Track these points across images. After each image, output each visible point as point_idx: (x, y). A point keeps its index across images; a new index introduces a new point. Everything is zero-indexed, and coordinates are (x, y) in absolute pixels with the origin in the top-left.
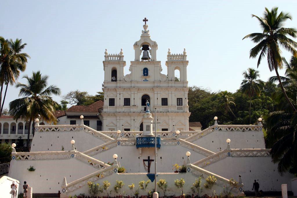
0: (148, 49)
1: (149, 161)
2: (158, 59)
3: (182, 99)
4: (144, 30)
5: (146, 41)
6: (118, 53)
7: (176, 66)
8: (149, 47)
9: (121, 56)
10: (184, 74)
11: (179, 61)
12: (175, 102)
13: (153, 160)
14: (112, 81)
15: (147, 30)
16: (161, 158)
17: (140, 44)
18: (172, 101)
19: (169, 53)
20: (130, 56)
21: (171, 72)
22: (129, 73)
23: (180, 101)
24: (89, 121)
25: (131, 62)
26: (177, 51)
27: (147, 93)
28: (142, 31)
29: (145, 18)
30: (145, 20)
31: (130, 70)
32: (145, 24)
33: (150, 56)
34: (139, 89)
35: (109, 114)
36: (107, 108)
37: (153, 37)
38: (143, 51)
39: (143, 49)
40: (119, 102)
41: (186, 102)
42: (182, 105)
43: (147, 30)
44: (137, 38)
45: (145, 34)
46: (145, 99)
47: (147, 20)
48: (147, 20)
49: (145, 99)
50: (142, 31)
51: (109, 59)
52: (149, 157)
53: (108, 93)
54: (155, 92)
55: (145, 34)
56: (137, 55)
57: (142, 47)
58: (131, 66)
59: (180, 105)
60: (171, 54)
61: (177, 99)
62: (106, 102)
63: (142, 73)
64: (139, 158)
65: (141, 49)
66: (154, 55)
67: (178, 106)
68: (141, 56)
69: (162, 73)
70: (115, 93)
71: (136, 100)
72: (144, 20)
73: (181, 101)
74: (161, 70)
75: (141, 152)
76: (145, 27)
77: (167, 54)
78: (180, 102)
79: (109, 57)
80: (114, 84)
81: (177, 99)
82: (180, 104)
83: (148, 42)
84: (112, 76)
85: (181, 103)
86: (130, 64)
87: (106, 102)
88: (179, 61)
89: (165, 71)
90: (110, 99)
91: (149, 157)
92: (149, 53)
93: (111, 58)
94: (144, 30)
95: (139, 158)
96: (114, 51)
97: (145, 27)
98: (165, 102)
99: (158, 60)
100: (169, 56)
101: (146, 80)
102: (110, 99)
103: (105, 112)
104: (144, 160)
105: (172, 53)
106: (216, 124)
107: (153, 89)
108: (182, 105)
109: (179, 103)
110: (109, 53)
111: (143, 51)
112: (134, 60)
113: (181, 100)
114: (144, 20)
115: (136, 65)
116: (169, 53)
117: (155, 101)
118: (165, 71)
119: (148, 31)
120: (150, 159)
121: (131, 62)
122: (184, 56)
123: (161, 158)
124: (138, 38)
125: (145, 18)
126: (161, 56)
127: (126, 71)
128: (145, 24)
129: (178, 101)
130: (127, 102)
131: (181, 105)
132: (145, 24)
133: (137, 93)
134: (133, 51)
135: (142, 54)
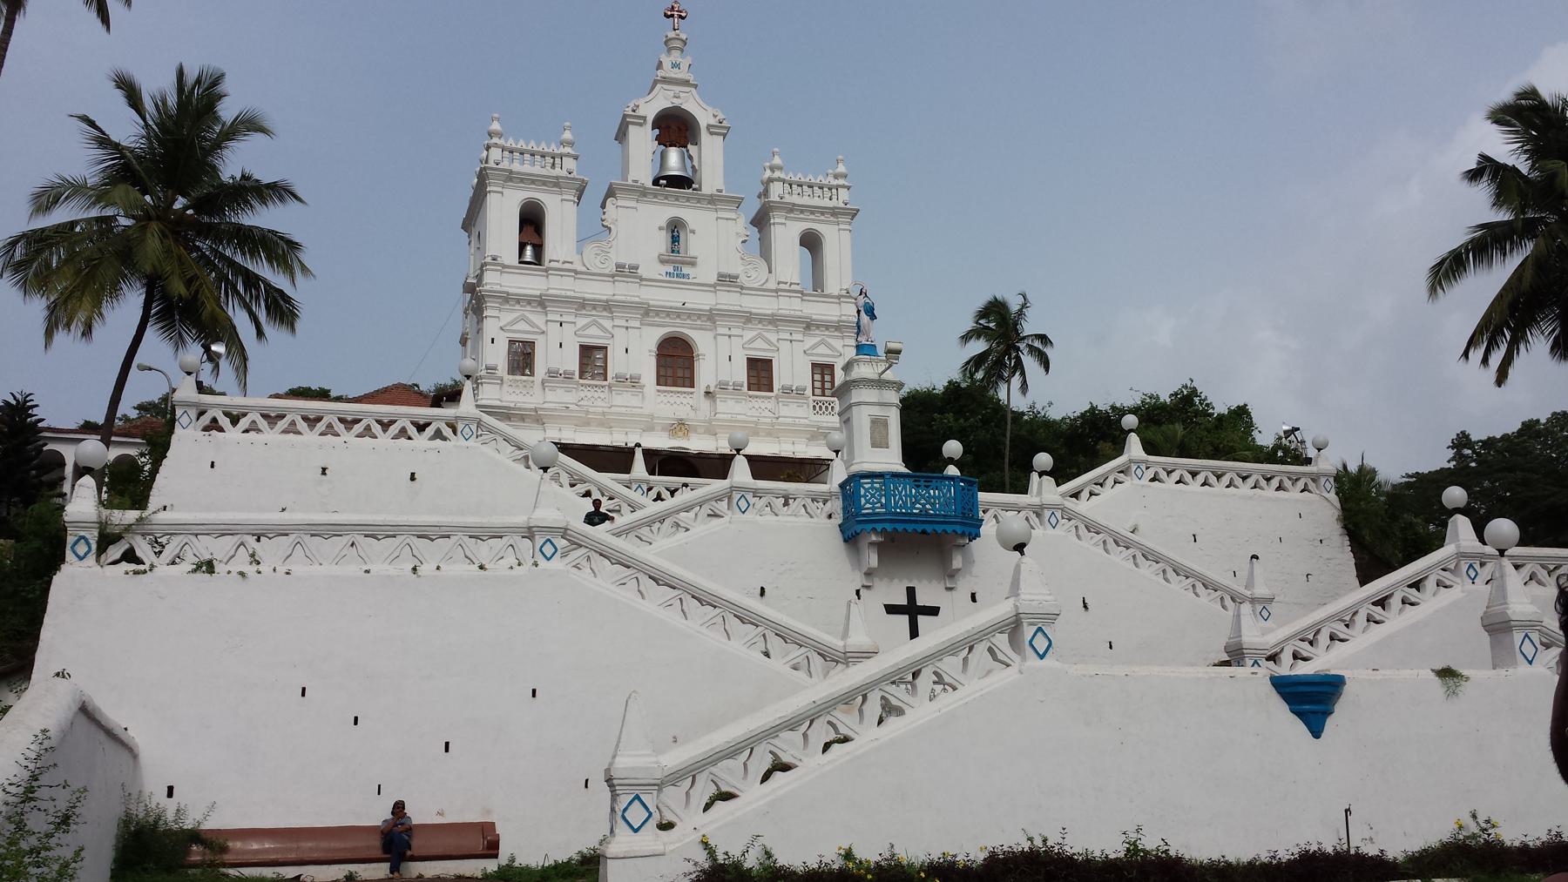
5: (677, 102)
13: (934, 611)
34: (647, 312)
52: (911, 592)
53: (507, 317)
54: (721, 330)
61: (814, 365)
63: (661, 242)
64: (858, 592)
70: (538, 319)
73: (827, 378)
78: (823, 381)
81: (814, 365)
82: (823, 389)
91: (911, 592)
95: (858, 592)
98: (760, 373)
104: (891, 609)
106: (1134, 446)
107: (711, 317)
109: (818, 384)
129: (817, 377)
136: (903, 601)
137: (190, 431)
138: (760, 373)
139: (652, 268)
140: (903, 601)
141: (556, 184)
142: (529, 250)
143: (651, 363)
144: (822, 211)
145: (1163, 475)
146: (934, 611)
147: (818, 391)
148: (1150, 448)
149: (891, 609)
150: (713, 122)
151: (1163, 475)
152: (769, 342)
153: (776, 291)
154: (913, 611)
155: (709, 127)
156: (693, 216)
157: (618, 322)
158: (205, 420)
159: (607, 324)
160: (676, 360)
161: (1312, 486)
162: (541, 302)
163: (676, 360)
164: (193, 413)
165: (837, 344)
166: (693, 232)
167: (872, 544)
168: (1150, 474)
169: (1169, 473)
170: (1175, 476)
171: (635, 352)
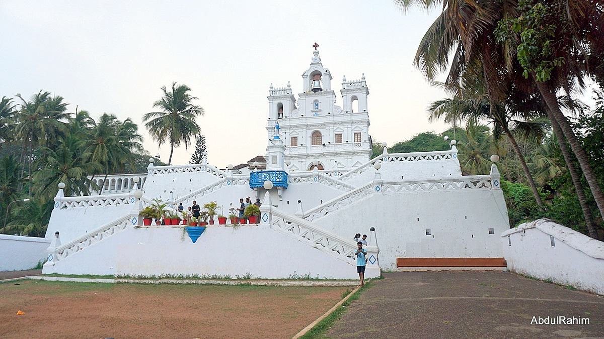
5: (316, 69)
11: (357, 90)
12: (351, 139)
30: (316, 46)
37: (327, 64)
44: (306, 67)
45: (317, 62)
55: (317, 62)
63: (311, 107)
76: (316, 53)
84: (279, 114)
88: (357, 90)
94: (314, 57)
96: (280, 84)
97: (316, 53)
98: (339, 138)
110: (275, 87)
115: (305, 98)
117: (328, 136)
118: (340, 101)
128: (316, 50)
132: (316, 50)
133: (305, 130)
138: (339, 138)
141: (285, 97)
142: (281, 115)
143: (309, 140)
144: (357, 90)
145: (395, 159)
151: (395, 159)
152: (297, 133)
158: (154, 172)
159: (297, 131)
160: (316, 137)
161: (449, 157)
163: (316, 137)
165: (362, 126)
168: (390, 159)
169: (397, 159)
170: (399, 159)
171: (305, 137)
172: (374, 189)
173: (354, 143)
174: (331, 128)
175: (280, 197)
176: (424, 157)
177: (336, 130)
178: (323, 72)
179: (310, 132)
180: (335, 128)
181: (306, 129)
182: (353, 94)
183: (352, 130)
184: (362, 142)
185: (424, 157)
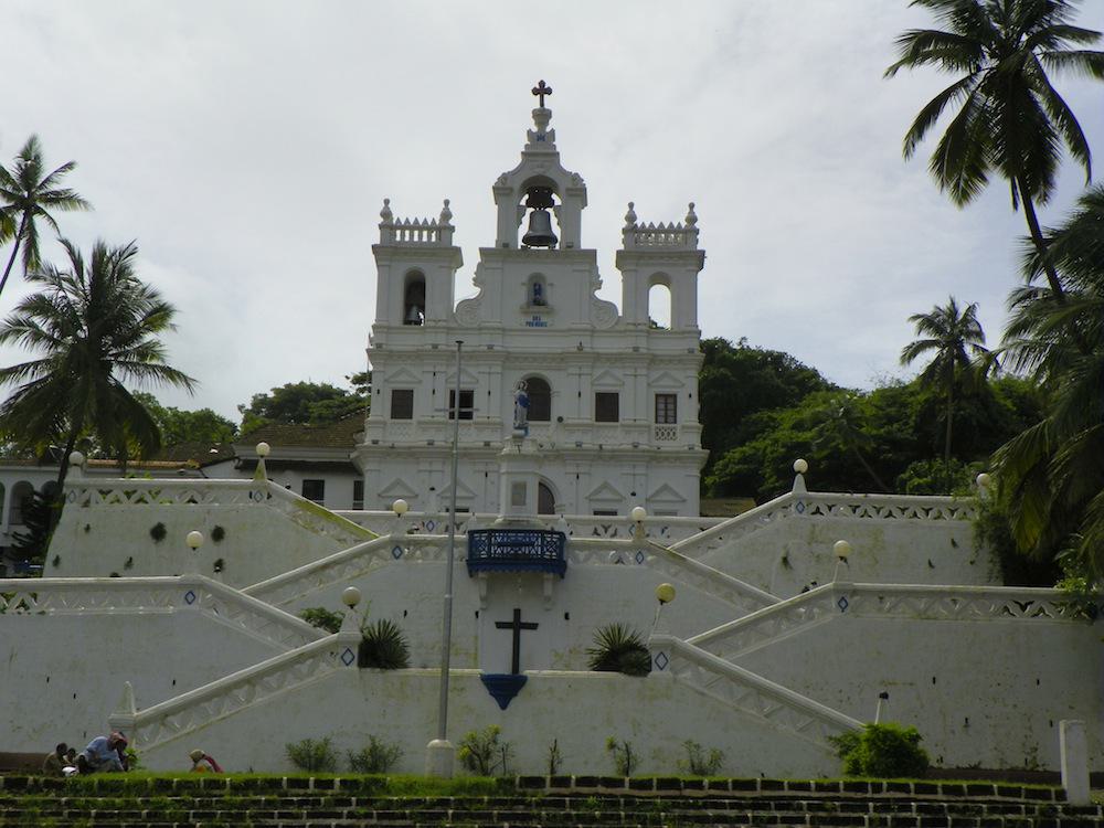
0: (551, 203)
1: (517, 625)
2: (586, 243)
3: (675, 396)
4: (535, 129)
6: (433, 214)
7: (651, 271)
8: (554, 196)
9: (444, 228)
10: (685, 304)
11: (666, 254)
13: (533, 626)
14: (407, 322)
15: (548, 129)
16: (567, 617)
17: (517, 185)
18: (636, 406)
19: (631, 218)
20: (476, 230)
21: (636, 296)
22: (472, 292)
23: (666, 405)
24: (323, 482)
25: (483, 251)
26: (658, 212)
27: (538, 371)
28: (529, 132)
29: (542, 84)
30: (542, 90)
31: (477, 282)
32: (538, 106)
33: (556, 230)
34: (508, 358)
35: (392, 452)
36: (379, 427)
37: (571, 159)
38: (532, 210)
39: (529, 204)
40: (430, 404)
41: (688, 411)
42: (675, 422)
43: (548, 129)
45: (541, 144)
46: (536, 400)
47: (549, 91)
48: (549, 91)
49: (536, 400)
50: (529, 132)
51: (398, 238)
52: (517, 612)
55: (541, 144)
56: (507, 223)
57: (527, 197)
58: (479, 265)
59: (666, 422)
60: (639, 223)
61: (657, 396)
62: (380, 409)
64: (477, 613)
65: (523, 203)
66: (572, 224)
67: (658, 425)
68: (523, 230)
69: (599, 294)
71: (497, 402)
72: (535, 92)
73: (671, 406)
74: (599, 285)
75: (484, 593)
76: (542, 116)
77: (624, 224)
79: (398, 232)
80: (410, 340)
81: (657, 396)
82: (666, 416)
83: (551, 174)
84: (408, 307)
85: (671, 413)
86: (478, 259)
87: (380, 409)
88: (666, 254)
89: (611, 287)
90: (395, 392)
91: (517, 612)
92: (554, 220)
93: (403, 235)
94: (535, 129)
95: (477, 613)
96: (416, 207)
97: (542, 116)
98: (607, 407)
99: (585, 245)
100: (632, 230)
101: (536, 322)
102: (395, 392)
103: (375, 442)
104: (500, 625)
105: (643, 219)
107: (561, 359)
108: (675, 422)
109: (662, 413)
110: (400, 214)
111: (530, 210)
112: (493, 245)
113: (670, 400)
114: (535, 92)
115: (499, 265)
116: (631, 218)
117: (571, 400)
118: (611, 287)
119: (553, 131)
120: (523, 620)
121: (483, 251)
122: (690, 230)
123: (567, 617)
124: (512, 161)
125: (542, 84)
126: (601, 232)
127: (464, 286)
128: (542, 104)
129: (662, 406)
130: (463, 403)
131: (671, 419)
132: (542, 104)
133: (499, 369)
134: (492, 210)
135: (526, 220)
136: (509, 618)
137: (75, 504)
139: (519, 321)
140: (509, 618)
142: (415, 309)
146: (533, 626)
147: (661, 419)
148: (810, 486)
149: (500, 625)
150: (570, 186)
153: (625, 331)
154: (517, 625)
155: (568, 190)
156: (550, 272)
157: (482, 369)
162: (417, 356)
164: (77, 491)
166: (552, 285)
167: (482, 578)
172: (833, 602)
173: (654, 425)
174: (585, 370)
175: (548, 599)
176: (903, 510)
177: (600, 377)
178: (563, 184)
179: (517, 376)
180: (598, 372)
181: (503, 368)
182: (658, 269)
183: (649, 385)
184: (678, 426)
185: (903, 510)
